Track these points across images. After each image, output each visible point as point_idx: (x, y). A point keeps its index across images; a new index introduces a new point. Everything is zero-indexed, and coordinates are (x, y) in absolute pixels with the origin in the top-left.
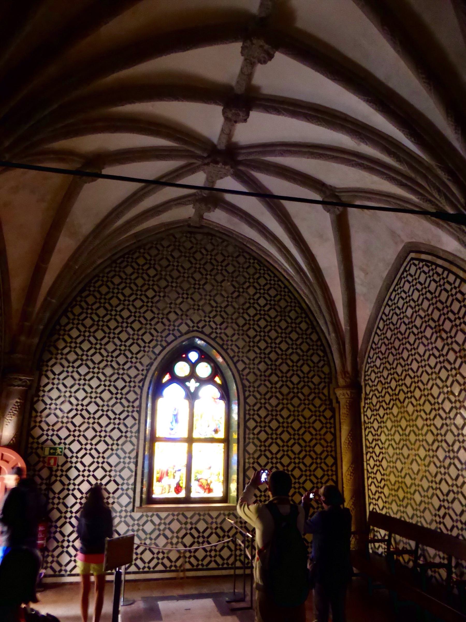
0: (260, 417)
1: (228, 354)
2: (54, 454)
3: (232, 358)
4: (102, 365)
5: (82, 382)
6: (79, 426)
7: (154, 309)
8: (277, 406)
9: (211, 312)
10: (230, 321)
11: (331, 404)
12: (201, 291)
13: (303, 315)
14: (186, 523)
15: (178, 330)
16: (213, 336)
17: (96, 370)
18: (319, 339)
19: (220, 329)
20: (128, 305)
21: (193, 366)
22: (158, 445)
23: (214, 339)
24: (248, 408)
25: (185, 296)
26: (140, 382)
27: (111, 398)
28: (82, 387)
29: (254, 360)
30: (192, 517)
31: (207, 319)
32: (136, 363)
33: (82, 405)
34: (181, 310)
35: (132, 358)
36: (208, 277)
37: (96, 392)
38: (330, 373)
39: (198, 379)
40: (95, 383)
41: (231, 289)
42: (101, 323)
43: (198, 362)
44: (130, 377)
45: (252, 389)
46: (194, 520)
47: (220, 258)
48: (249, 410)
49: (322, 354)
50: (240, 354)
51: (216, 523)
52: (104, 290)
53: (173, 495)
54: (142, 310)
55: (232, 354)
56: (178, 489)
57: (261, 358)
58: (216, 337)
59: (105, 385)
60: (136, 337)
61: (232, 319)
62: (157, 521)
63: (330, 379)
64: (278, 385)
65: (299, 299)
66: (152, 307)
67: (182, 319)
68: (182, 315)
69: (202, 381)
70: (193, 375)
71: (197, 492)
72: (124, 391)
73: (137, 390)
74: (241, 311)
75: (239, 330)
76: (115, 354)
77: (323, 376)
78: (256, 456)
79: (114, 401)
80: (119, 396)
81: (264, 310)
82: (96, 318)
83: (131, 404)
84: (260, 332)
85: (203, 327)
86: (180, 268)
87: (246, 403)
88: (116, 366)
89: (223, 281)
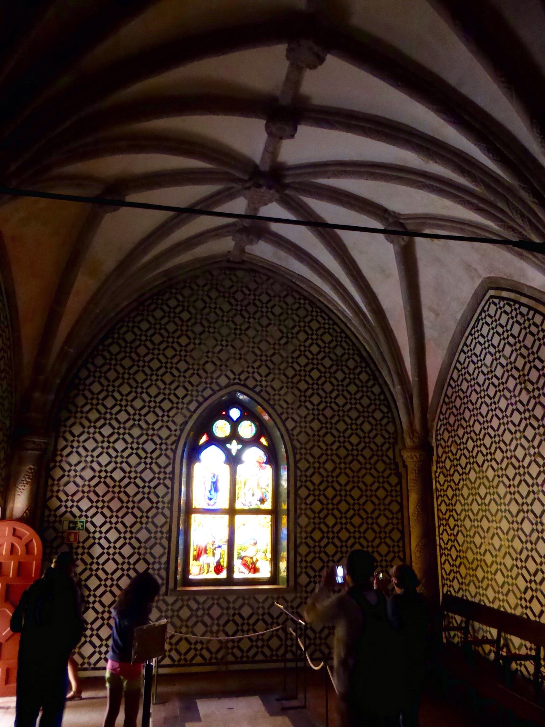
0: (313, 484)
1: (275, 411)
2: (74, 528)
3: (279, 416)
4: (128, 425)
5: (106, 445)
6: (103, 496)
7: (188, 359)
8: (333, 471)
9: (255, 361)
10: (277, 371)
11: (397, 469)
12: (243, 337)
13: (364, 365)
14: (228, 608)
15: (217, 383)
16: (258, 389)
17: (122, 431)
18: (382, 392)
19: (266, 381)
20: (158, 354)
21: (235, 425)
22: (195, 518)
23: (258, 394)
24: (299, 473)
25: (224, 343)
26: (172, 444)
27: (139, 463)
28: (105, 450)
29: (305, 417)
30: (234, 602)
31: (251, 370)
32: (168, 422)
33: (106, 471)
34: (220, 359)
35: (163, 416)
36: (251, 320)
37: (122, 457)
38: (396, 431)
39: (240, 440)
40: (120, 445)
41: (278, 335)
42: (126, 376)
43: (240, 420)
44: (161, 438)
45: (303, 451)
46: (237, 605)
47: (265, 298)
48: (301, 476)
49: (385, 410)
50: (290, 411)
51: (263, 608)
52: (129, 337)
53: (212, 575)
54: (175, 360)
55: (279, 410)
56: (218, 569)
57: (314, 415)
58: (261, 391)
60: (167, 391)
61: (280, 369)
62: (194, 606)
63: (396, 439)
64: (335, 447)
65: (358, 345)
66: (186, 356)
67: (221, 370)
68: (221, 366)
69: (245, 443)
70: (234, 435)
71: (240, 572)
72: (155, 455)
73: (169, 453)
74: (290, 360)
75: (287, 383)
76: (143, 412)
77: (387, 436)
78: (309, 529)
79: (142, 466)
80: (149, 461)
81: (317, 359)
82: (121, 371)
83: (162, 470)
84: (313, 384)
85: (246, 379)
86: (218, 311)
87: (296, 467)
88: (144, 426)
89: (269, 324)
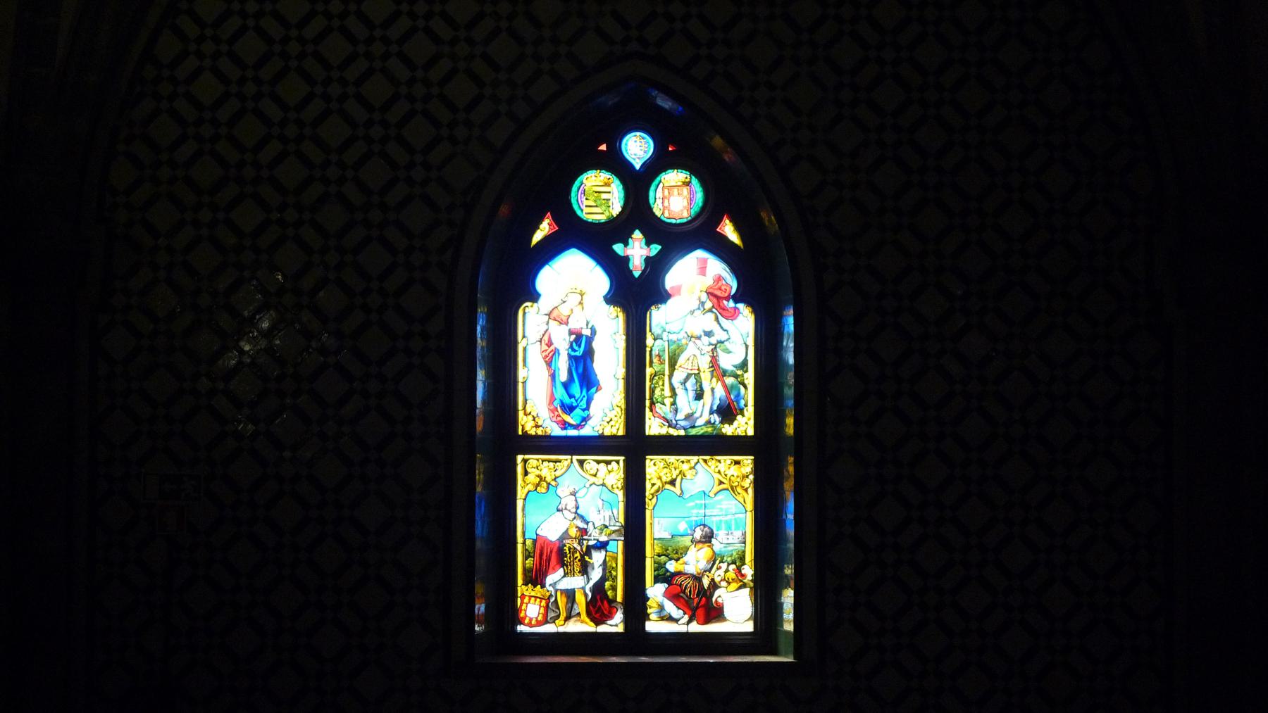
71: (665, 618)
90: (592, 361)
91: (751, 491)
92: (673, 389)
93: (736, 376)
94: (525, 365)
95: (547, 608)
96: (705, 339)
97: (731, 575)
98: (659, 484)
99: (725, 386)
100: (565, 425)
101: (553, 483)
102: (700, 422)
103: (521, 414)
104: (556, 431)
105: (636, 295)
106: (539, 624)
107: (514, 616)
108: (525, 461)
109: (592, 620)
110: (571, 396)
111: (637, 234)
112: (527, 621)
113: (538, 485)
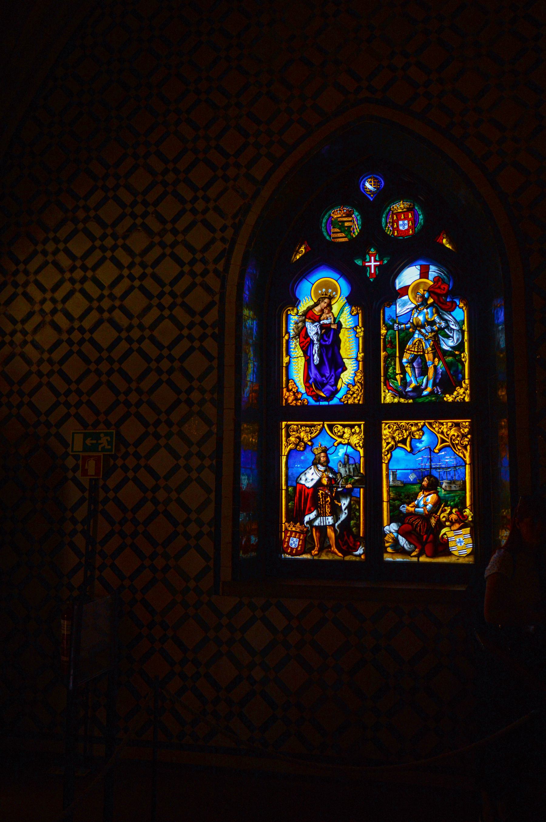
5: (78, 274)
27: (148, 308)
28: (78, 286)
40: (107, 273)
59: (131, 277)
72: (180, 287)
79: (155, 313)
88: (156, 226)
90: (339, 348)
91: (468, 447)
92: (402, 367)
93: (454, 356)
94: (288, 353)
95: (305, 541)
96: (428, 328)
97: (454, 517)
98: (393, 443)
99: (445, 363)
100: (318, 398)
101: (309, 443)
102: (425, 393)
103: (285, 390)
104: (312, 402)
105: (372, 297)
106: (298, 553)
107: (279, 545)
108: (287, 426)
109: (340, 552)
110: (323, 375)
111: (373, 251)
112: (289, 551)
113: (297, 445)
